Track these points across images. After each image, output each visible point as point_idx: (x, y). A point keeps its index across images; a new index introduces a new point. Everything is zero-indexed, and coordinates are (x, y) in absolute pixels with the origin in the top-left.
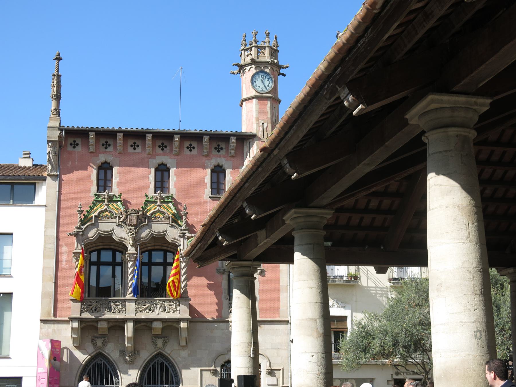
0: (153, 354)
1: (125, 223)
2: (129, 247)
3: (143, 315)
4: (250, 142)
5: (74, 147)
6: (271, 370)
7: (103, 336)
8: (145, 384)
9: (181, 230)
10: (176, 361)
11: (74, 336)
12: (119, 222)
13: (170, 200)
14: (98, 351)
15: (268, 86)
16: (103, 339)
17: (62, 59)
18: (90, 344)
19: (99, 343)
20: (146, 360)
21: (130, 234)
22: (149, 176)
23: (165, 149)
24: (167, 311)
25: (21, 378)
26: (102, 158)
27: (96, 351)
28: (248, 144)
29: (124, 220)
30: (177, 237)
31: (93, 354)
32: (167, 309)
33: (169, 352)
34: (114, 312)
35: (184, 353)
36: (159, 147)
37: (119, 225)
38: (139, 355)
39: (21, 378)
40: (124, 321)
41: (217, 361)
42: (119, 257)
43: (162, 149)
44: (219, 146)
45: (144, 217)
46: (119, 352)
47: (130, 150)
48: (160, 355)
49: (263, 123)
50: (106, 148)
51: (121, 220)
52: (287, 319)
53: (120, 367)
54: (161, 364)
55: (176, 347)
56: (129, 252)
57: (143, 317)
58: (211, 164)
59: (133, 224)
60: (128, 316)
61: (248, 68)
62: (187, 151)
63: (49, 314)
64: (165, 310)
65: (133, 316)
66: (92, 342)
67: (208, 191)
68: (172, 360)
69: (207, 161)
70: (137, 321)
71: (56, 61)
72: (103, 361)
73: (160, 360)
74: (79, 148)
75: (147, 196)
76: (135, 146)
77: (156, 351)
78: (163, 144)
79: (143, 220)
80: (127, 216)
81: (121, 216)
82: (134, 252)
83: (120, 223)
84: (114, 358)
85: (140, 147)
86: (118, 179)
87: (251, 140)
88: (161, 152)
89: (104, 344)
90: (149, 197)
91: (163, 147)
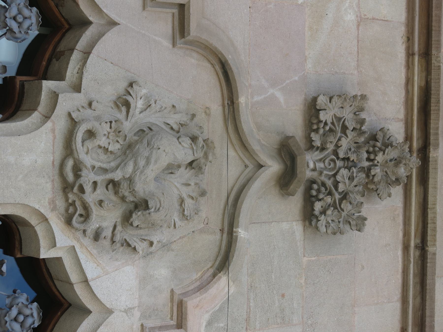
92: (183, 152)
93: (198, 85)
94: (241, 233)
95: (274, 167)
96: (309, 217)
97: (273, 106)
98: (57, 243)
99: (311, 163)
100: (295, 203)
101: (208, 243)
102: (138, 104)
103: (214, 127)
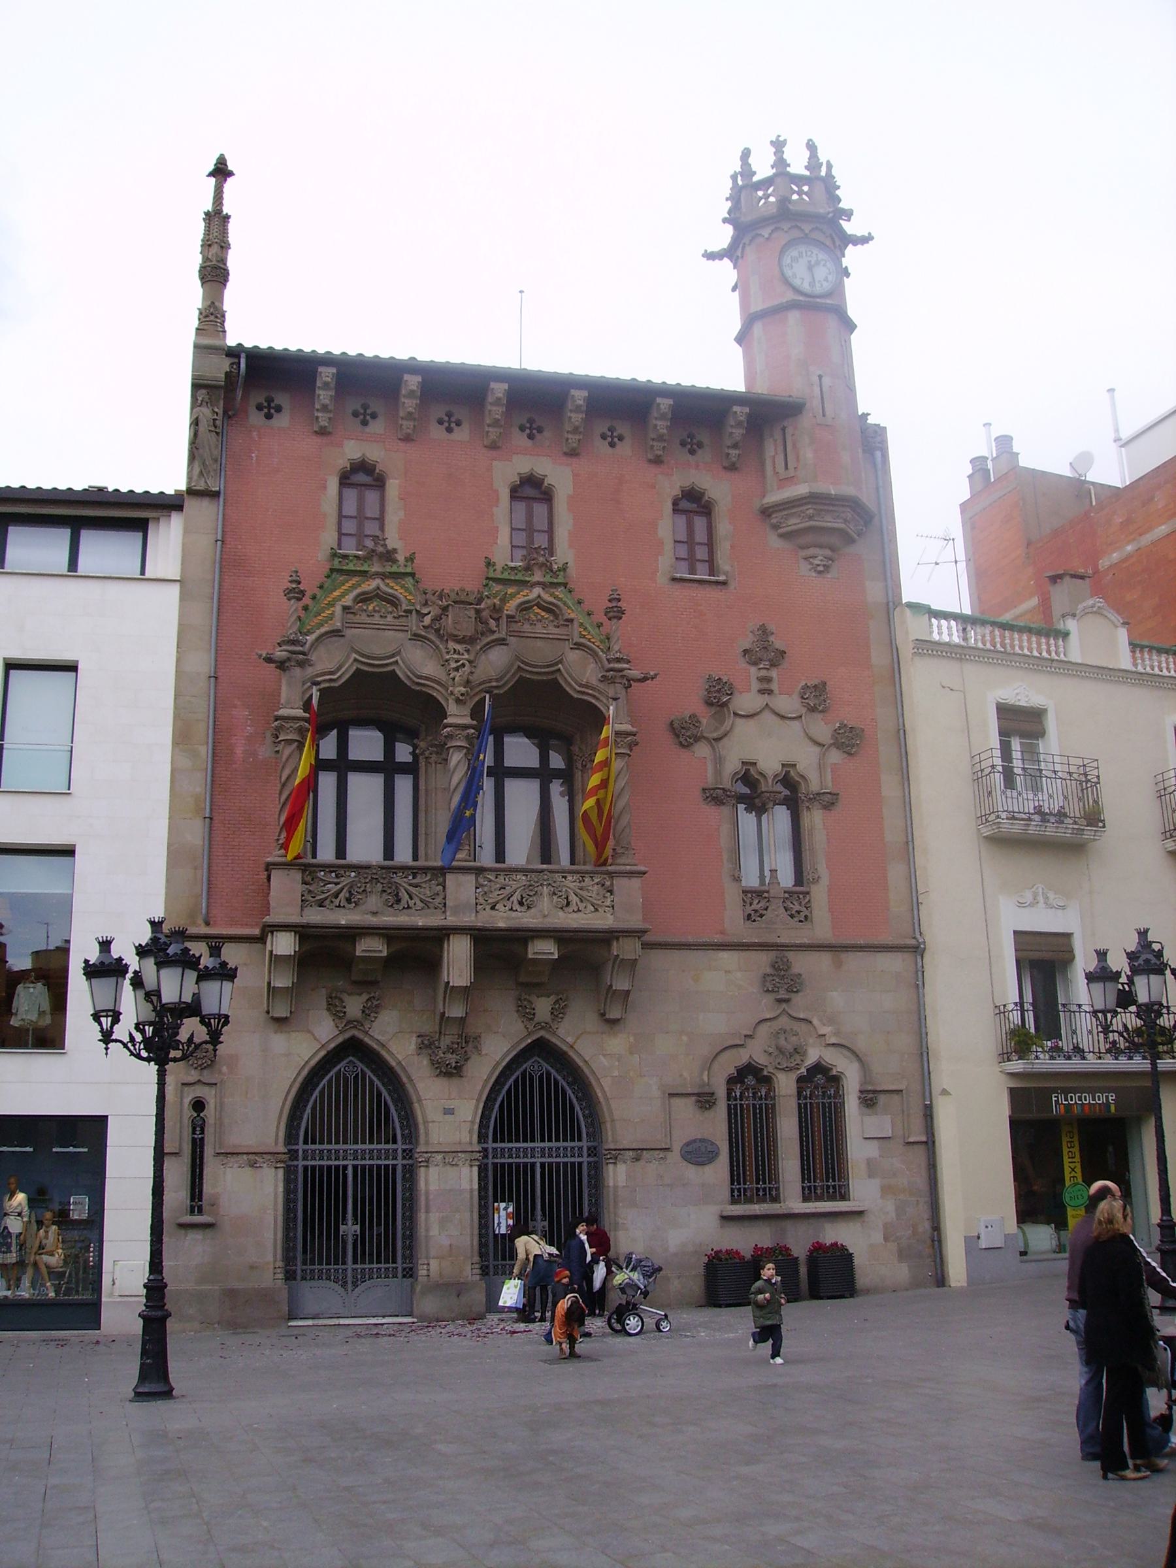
0: (523, 1046)
1: (437, 631)
2: (452, 708)
3: (502, 919)
4: (784, 429)
5: (269, 416)
6: (875, 1092)
7: (365, 985)
8: (495, 1141)
10: (594, 1066)
11: (279, 983)
13: (560, 580)
14: (347, 1035)
15: (826, 280)
16: (365, 997)
17: (231, 174)
18: (325, 1013)
19: (354, 1006)
20: (498, 1063)
21: (454, 665)
22: (495, 510)
23: (538, 436)
24: (573, 907)
25: (103, 1119)
26: (352, 450)
27: (341, 1032)
28: (778, 435)
31: (332, 1045)
32: (574, 899)
33: (570, 1040)
34: (409, 907)
35: (617, 1043)
36: (522, 429)
37: (416, 637)
38: (478, 1049)
39: (103, 1119)
40: (442, 935)
41: (716, 1066)
42: (403, 753)
43: (531, 437)
44: (691, 436)
45: (496, 616)
46: (414, 1039)
47: (437, 432)
48: (541, 1048)
49: (820, 377)
50: (365, 423)
51: (427, 620)
52: (913, 942)
53: (420, 1086)
54: (541, 1077)
55: (591, 1021)
56: (449, 720)
57: (501, 924)
59: (461, 634)
60: (451, 920)
61: (766, 232)
62: (603, 447)
63: (192, 916)
64: (568, 904)
67: (665, 562)
68: (581, 1064)
70: (482, 938)
71: (213, 180)
73: (537, 1066)
74: (282, 421)
75: (489, 564)
76: (449, 422)
78: (531, 421)
79: (492, 623)
80: (445, 609)
81: (425, 611)
82: (467, 721)
85: (466, 426)
86: (402, 514)
87: (786, 424)
88: (529, 443)
89: (371, 1011)
90: (499, 567)
91: (532, 431)
92: (782, 1037)
93: (764, 1029)
94: (801, 1016)
95: (784, 1005)
96: (797, 992)
97: (766, 1007)
98: (803, 1070)
99: (782, 994)
100: (793, 995)
101: (803, 1026)
102: (771, 1050)
103: (776, 1025)
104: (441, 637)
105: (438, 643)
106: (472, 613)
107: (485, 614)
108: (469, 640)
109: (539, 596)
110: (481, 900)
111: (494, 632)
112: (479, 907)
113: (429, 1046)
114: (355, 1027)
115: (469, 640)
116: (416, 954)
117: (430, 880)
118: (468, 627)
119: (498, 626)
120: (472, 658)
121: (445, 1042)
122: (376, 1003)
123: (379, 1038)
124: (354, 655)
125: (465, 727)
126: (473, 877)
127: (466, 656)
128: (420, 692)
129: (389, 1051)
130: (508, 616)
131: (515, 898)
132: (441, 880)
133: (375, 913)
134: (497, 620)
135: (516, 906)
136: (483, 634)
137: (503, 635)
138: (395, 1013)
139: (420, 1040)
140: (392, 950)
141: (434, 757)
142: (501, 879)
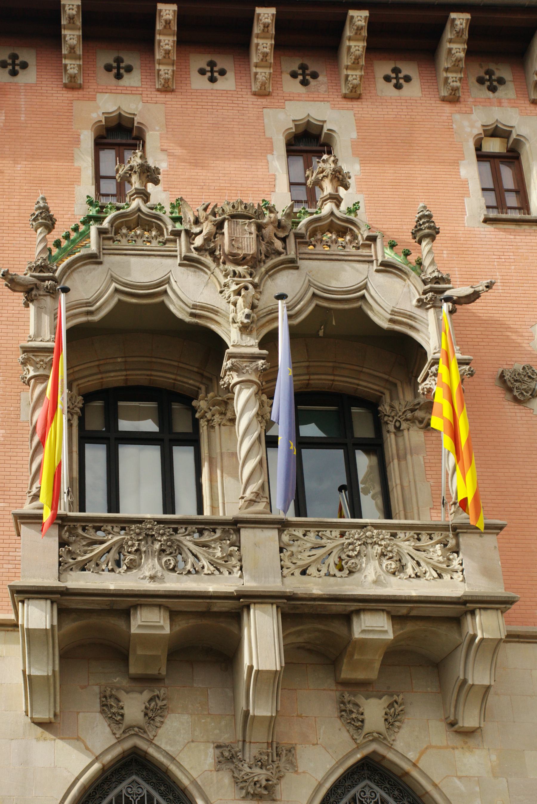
1: (212, 253)
9: (425, 282)
12: (189, 250)
21: (234, 287)
29: (207, 240)
30: (410, 305)
37: (189, 262)
40: (238, 606)
45: (282, 235)
51: (199, 241)
58: (472, 126)
59: (241, 253)
65: (273, 584)
66: (105, 707)
69: (457, 117)
72: (146, 788)
77: (359, 747)
79: (278, 244)
83: (195, 254)
84: (195, 774)
104: (216, 259)
105: (213, 265)
106: (253, 229)
107: (269, 231)
108: (253, 262)
109: (332, 214)
110: (287, 563)
111: (279, 254)
112: (285, 571)
113: (231, 759)
114: (136, 735)
115: (253, 262)
116: (207, 638)
117: (221, 539)
118: (249, 245)
119: (285, 248)
120: (256, 280)
121: (251, 752)
122: (160, 703)
123: (168, 748)
124: (114, 285)
125: (254, 358)
126: (275, 533)
127: (249, 279)
128: (197, 325)
129: (180, 766)
130: (298, 236)
131: (333, 559)
132: (234, 537)
133: (153, 578)
134: (284, 240)
135: (333, 570)
136: (267, 257)
137: (292, 254)
138: (186, 718)
139: (218, 752)
140: (177, 628)
141: (217, 418)
142: (312, 536)
